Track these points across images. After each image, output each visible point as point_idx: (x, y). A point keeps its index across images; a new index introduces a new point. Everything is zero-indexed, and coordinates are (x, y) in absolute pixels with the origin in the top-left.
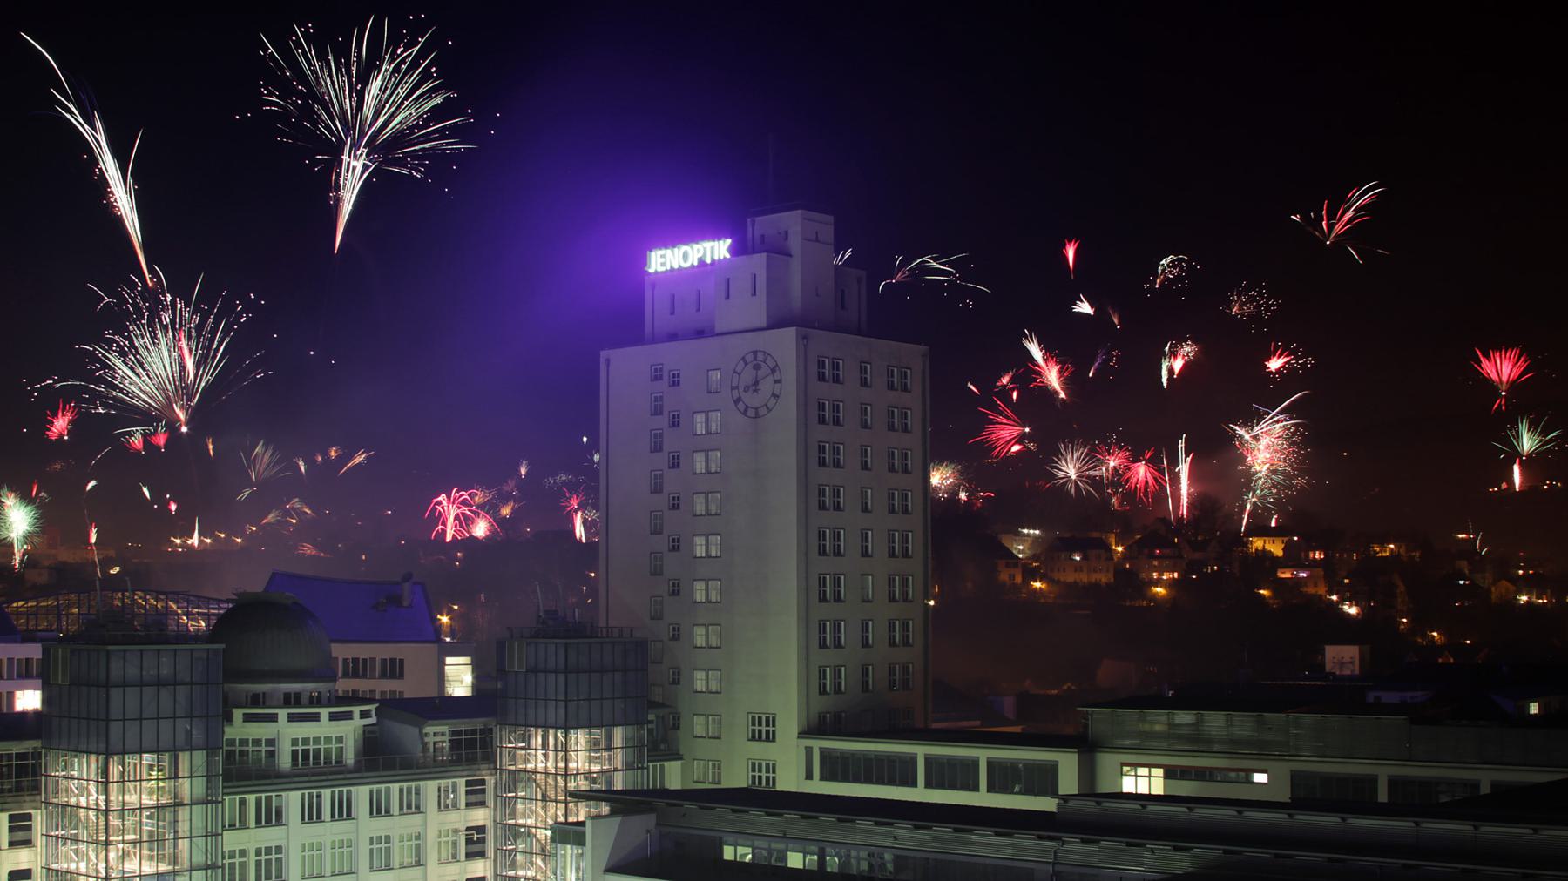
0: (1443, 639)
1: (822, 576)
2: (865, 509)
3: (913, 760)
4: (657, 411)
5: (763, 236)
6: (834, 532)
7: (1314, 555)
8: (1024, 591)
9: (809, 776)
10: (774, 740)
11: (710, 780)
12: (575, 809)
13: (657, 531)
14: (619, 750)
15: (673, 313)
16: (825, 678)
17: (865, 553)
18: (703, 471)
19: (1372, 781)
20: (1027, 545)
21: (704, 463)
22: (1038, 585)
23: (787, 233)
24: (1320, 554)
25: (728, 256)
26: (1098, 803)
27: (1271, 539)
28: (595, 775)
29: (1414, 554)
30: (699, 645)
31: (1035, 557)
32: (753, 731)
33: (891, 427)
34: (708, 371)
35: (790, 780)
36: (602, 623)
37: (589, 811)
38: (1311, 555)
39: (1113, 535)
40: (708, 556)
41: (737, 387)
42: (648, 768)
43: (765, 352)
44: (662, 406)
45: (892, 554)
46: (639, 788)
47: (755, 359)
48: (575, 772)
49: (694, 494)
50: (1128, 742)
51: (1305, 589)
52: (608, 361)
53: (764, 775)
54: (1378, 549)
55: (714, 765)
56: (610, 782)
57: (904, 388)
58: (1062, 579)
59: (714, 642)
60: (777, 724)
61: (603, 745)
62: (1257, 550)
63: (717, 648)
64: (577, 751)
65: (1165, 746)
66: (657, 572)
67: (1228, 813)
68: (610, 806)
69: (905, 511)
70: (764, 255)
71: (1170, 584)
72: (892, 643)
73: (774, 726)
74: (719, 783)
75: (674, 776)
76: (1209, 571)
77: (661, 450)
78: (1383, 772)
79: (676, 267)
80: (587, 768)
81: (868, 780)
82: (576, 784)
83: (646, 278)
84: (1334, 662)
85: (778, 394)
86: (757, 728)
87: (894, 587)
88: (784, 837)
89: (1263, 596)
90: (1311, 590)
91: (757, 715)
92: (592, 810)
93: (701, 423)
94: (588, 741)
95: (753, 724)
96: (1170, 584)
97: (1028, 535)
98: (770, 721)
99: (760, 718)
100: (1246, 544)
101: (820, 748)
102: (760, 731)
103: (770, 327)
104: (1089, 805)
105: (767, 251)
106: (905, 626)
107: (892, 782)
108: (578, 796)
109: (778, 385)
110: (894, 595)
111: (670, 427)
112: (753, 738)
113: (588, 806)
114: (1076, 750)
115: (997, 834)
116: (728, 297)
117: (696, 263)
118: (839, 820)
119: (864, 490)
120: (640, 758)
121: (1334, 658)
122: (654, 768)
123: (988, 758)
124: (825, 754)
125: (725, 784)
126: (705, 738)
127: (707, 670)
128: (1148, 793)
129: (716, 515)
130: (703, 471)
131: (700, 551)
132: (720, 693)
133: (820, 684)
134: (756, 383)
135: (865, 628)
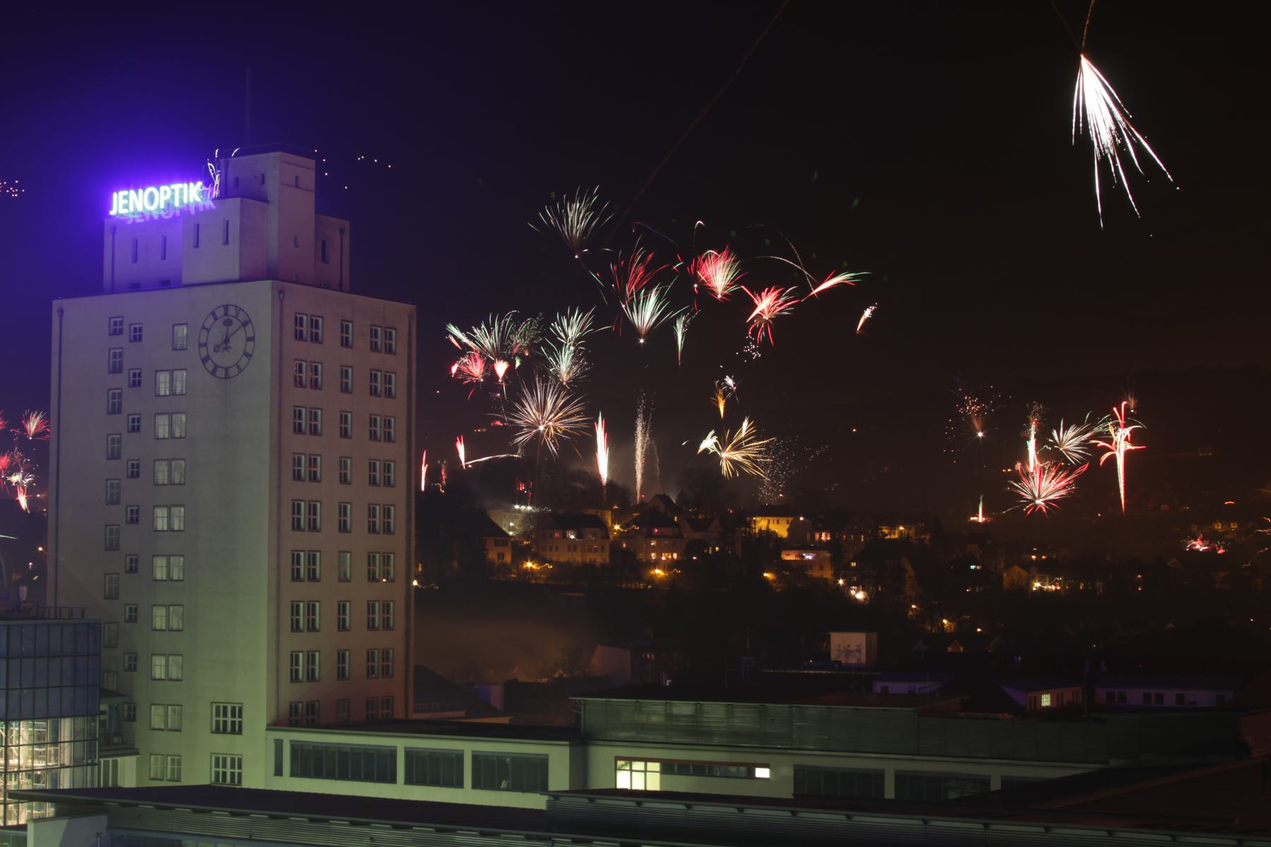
0: (952, 626)
1: (296, 553)
2: (344, 480)
3: (392, 753)
4: (116, 369)
5: (237, 179)
6: (310, 505)
7: (821, 536)
8: (513, 571)
9: (279, 772)
10: (240, 732)
11: (169, 776)
12: (15, 811)
13: (114, 501)
14: (66, 744)
15: (135, 261)
16: (297, 664)
17: (343, 528)
18: (167, 436)
19: (880, 775)
20: (518, 521)
21: (167, 427)
22: (529, 565)
23: (263, 176)
24: (826, 536)
25: (198, 199)
26: (591, 800)
27: (776, 519)
28: (39, 773)
29: (923, 536)
30: (158, 627)
31: (526, 535)
32: (218, 722)
33: (374, 392)
34: (174, 325)
35: (257, 777)
36: (50, 603)
37: (32, 814)
38: (817, 536)
39: (610, 513)
40: (171, 529)
41: (205, 345)
42: (99, 764)
43: (236, 306)
44: (121, 363)
45: (372, 529)
46: (89, 786)
47: (226, 314)
48: (16, 770)
49: (155, 460)
50: (623, 735)
51: (809, 573)
52: (61, 311)
53: (229, 771)
54: (886, 531)
55: (173, 761)
56: (55, 780)
57: (389, 350)
58: (555, 559)
59: (175, 626)
60: (244, 713)
61: (48, 739)
62: (760, 530)
63: (178, 630)
64: (19, 745)
65: (661, 738)
66: (113, 546)
67: (729, 810)
68: (56, 808)
69: (388, 483)
70: (238, 200)
71: (668, 566)
72: (371, 626)
73: (240, 716)
74: (179, 780)
75: (128, 773)
76: (710, 552)
77: (119, 412)
78: (890, 767)
79: (140, 209)
80: (30, 764)
81: (343, 776)
82: (16, 783)
83: (106, 221)
84: (840, 651)
85: (251, 353)
86: (221, 719)
87: (374, 565)
88: (250, 839)
89: (767, 578)
90: (816, 573)
91: (222, 705)
92: (34, 812)
93: (165, 383)
94: (32, 735)
95: (218, 715)
96: (668, 566)
97: (519, 511)
98: (238, 712)
99: (225, 708)
100: (749, 525)
101: (291, 741)
102: (225, 722)
103: (242, 280)
104: (582, 801)
105: (243, 196)
106: (386, 608)
107: (369, 778)
108: (20, 796)
109: (250, 344)
110: (374, 573)
111: (130, 386)
112: (217, 731)
113: (30, 808)
114: (568, 743)
115: (483, 834)
116: (197, 245)
117: (162, 206)
118: (312, 820)
119: (343, 459)
120: (91, 754)
121: (840, 646)
122: (106, 763)
123: (473, 751)
124: (297, 749)
125: (187, 780)
126: (163, 730)
127: (167, 656)
128: (643, 788)
129: (180, 484)
130: (167, 436)
131: (161, 524)
132: (181, 680)
133: (292, 670)
134: (227, 341)
135: (342, 609)
